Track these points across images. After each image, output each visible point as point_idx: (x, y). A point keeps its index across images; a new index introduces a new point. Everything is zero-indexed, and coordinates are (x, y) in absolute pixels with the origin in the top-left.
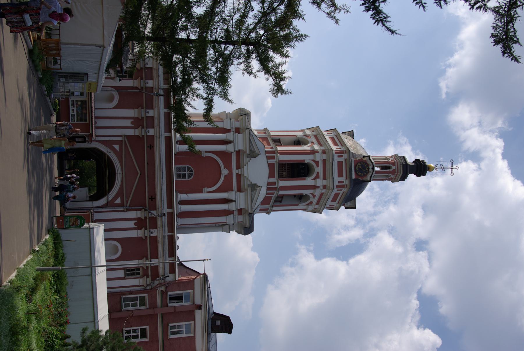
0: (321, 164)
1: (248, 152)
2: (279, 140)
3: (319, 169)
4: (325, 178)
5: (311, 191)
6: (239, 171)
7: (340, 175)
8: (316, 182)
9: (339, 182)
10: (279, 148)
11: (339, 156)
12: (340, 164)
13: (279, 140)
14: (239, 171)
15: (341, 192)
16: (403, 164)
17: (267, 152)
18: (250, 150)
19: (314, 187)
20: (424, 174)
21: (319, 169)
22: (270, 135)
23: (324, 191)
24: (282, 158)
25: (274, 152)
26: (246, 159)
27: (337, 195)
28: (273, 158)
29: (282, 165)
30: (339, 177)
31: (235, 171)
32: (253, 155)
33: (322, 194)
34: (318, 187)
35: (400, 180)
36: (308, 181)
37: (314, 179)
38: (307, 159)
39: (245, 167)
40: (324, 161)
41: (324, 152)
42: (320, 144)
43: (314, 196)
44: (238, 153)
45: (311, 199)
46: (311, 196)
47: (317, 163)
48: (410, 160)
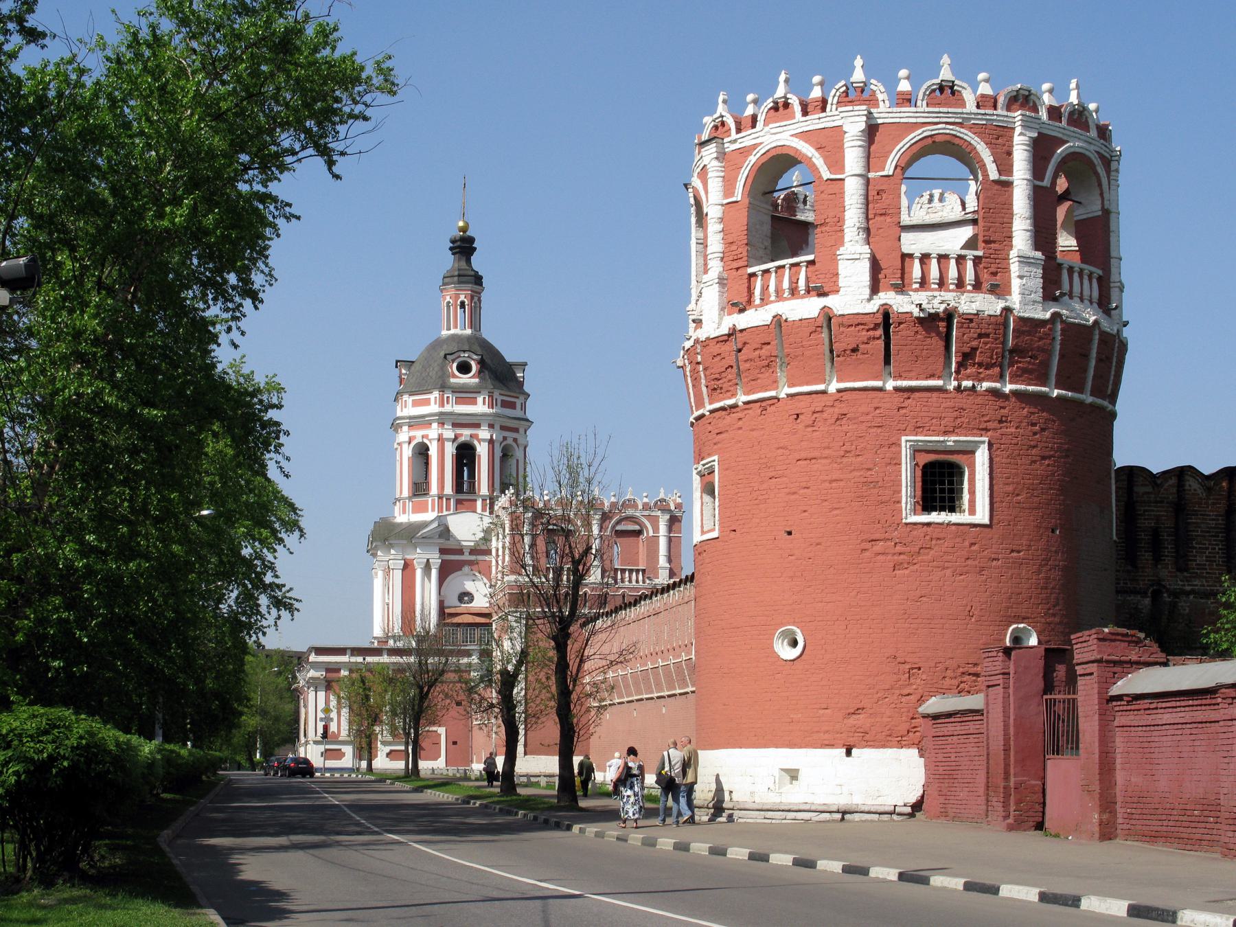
0: (459, 431)
1: (441, 541)
2: (415, 484)
3: (465, 434)
4: (477, 426)
5: (497, 446)
6: (467, 553)
7: (473, 402)
8: (484, 440)
9: (484, 403)
10: (434, 490)
11: (448, 403)
12: (459, 401)
13: (415, 484)
14: (467, 553)
15: (500, 398)
16: (460, 282)
17: (440, 510)
18: (440, 536)
19: (491, 442)
20: (471, 240)
21: (465, 434)
22: (410, 498)
23: (497, 427)
24: (449, 490)
25: (440, 498)
26: (450, 544)
27: (505, 404)
28: (448, 500)
29: (458, 487)
30: (475, 403)
31: (467, 557)
32: (445, 532)
33: (503, 428)
34: (492, 436)
35: (481, 284)
36: (482, 450)
37: (479, 441)
38: (450, 450)
39: (464, 543)
40: (455, 425)
41: (442, 424)
42: (429, 424)
43: (505, 438)
44: (443, 551)
45: (510, 441)
46: (505, 443)
47: (456, 437)
48: (448, 261)
